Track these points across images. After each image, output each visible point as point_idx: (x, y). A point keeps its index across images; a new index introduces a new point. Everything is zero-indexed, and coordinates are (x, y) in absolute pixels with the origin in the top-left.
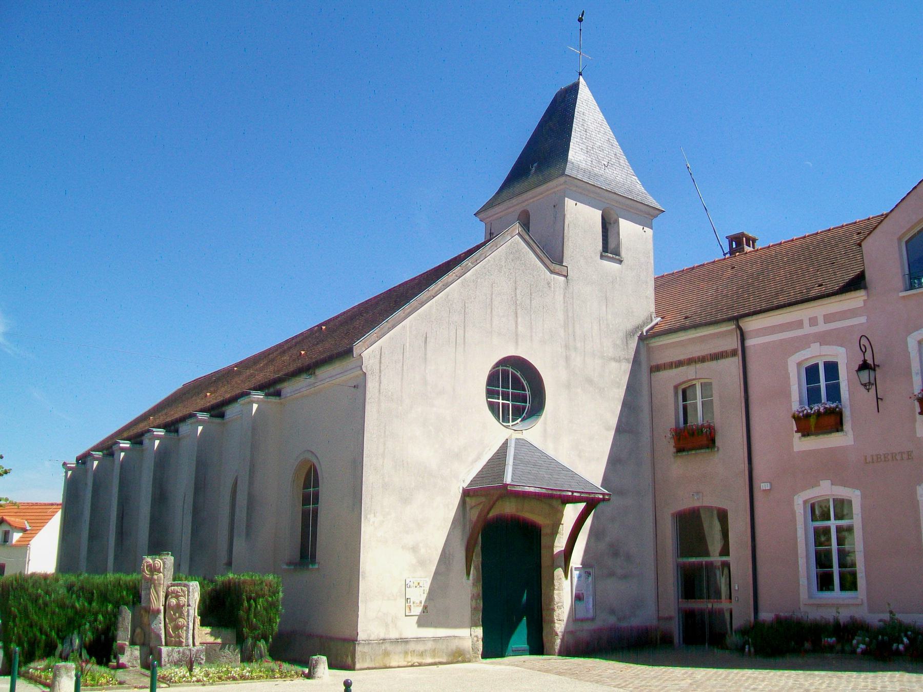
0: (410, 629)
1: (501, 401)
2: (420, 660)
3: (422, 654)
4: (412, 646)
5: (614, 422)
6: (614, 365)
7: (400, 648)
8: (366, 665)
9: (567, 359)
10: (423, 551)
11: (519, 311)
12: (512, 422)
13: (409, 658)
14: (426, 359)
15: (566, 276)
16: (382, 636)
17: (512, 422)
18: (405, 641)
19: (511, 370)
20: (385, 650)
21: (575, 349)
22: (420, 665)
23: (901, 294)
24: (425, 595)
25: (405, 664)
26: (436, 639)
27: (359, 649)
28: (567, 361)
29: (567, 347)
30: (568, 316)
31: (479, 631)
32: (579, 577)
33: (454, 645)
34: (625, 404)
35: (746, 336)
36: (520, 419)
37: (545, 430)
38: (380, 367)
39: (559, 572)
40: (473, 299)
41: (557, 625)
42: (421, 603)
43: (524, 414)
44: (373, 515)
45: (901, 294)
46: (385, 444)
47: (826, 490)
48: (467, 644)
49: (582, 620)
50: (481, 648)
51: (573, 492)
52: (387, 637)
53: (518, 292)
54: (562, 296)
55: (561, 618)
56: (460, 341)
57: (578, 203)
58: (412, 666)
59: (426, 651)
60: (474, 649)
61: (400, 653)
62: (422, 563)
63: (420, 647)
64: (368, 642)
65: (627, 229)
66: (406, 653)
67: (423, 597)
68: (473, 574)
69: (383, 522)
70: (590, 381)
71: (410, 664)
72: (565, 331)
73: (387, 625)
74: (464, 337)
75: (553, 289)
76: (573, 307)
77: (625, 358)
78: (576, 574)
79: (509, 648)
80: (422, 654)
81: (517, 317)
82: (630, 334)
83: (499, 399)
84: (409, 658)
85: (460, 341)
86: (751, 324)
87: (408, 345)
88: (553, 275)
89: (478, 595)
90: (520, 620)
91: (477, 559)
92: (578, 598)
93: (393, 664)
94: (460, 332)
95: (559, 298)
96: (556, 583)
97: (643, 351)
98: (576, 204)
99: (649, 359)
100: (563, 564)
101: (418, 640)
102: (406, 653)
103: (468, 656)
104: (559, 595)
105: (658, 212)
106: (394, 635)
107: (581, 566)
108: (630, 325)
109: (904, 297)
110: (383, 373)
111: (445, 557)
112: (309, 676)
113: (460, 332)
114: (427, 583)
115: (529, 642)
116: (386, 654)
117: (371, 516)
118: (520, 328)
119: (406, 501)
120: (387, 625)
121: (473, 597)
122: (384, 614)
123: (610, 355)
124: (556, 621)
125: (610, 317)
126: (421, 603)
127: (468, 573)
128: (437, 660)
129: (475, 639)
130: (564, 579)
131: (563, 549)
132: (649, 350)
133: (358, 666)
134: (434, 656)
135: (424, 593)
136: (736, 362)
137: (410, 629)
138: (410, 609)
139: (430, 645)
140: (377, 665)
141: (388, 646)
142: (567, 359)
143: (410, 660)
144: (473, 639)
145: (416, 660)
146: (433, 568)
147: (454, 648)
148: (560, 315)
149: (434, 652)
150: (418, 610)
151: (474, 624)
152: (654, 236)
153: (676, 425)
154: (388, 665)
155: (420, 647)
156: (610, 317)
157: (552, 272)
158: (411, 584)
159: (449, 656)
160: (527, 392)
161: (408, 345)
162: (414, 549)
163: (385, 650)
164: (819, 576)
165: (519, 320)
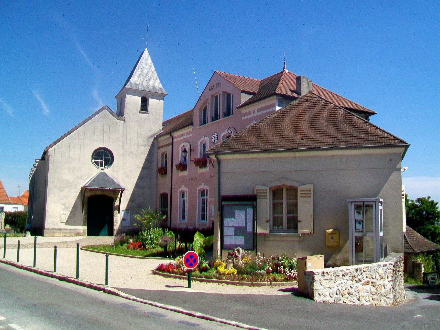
0: (63, 226)
1: (100, 161)
2: (65, 235)
3: (66, 233)
4: (62, 231)
5: (141, 165)
6: (143, 148)
7: (58, 231)
8: (47, 235)
9: (123, 147)
10: (67, 205)
11: (105, 134)
12: (104, 167)
13: (62, 234)
14: (70, 150)
15: (124, 121)
16: (53, 228)
17: (104, 167)
18: (60, 229)
19: (104, 151)
20: (54, 231)
21: (127, 143)
22: (65, 236)
23: (198, 127)
24: (67, 217)
25: (60, 235)
26: (71, 229)
27: (45, 231)
28: (123, 148)
29: (123, 143)
30: (124, 133)
31: (86, 228)
32: (124, 213)
33: (77, 231)
34: (146, 160)
35: (174, 138)
36: (107, 166)
37: (113, 169)
38: (54, 153)
39: (116, 212)
40: (87, 131)
41: (115, 227)
42: (66, 219)
43: (109, 164)
44: (51, 195)
45: (198, 127)
46: (55, 175)
47: (203, 186)
48: (82, 231)
49: (124, 226)
50: (87, 232)
51: (109, 188)
52: (54, 228)
53: (105, 127)
54: (122, 127)
55: (116, 225)
56: (82, 144)
57: (131, 96)
58: (62, 236)
59: (67, 232)
60: (84, 233)
61: (58, 233)
62: (67, 208)
63: (65, 231)
64: (48, 229)
65: (152, 102)
66: (60, 233)
67: (67, 218)
68: (84, 212)
69: (54, 197)
70: (132, 153)
71: (62, 236)
72: (123, 138)
73: (54, 225)
74: (84, 143)
75: (118, 125)
76: (127, 130)
77: (148, 145)
78: (123, 213)
79: (101, 234)
80: (66, 233)
81: (104, 135)
82: (151, 137)
83: (99, 160)
84: (62, 234)
85: (82, 144)
86: (175, 134)
87: (64, 146)
88: (119, 121)
89: (86, 218)
90: (105, 225)
91: (85, 208)
92: (123, 220)
93: (56, 235)
94: (82, 141)
95: (121, 128)
96: (115, 215)
97: (155, 142)
98: (130, 96)
99: (158, 144)
100: (118, 209)
101: (65, 229)
102: (60, 233)
103: (82, 234)
104: (116, 218)
105: (166, 95)
106: (57, 227)
107: (125, 210)
108: (151, 134)
109: (199, 128)
110: (55, 155)
111: (75, 207)
112: (25, 237)
113: (82, 141)
114: (68, 214)
115: (108, 232)
116: (54, 232)
117: (50, 196)
118: (105, 139)
119: (62, 191)
120: (54, 225)
121: (84, 218)
122: (54, 222)
123: (141, 144)
124: (114, 226)
125: (142, 132)
126: (66, 219)
127: (83, 211)
128: (71, 235)
129: (85, 230)
130: (118, 214)
131: (118, 205)
132: (158, 141)
133: (45, 235)
134: (70, 234)
135: (67, 216)
136: (171, 146)
137: (63, 226)
138: (62, 221)
139: (68, 231)
140: (51, 235)
141: (55, 231)
142: (123, 147)
143: (62, 234)
144: (83, 230)
145: (64, 235)
146: (70, 210)
147: (77, 232)
148: (121, 133)
149: (70, 233)
150: (65, 221)
151: (84, 225)
152: (164, 103)
153: (161, 166)
154: (54, 236)
155: (65, 231)
156: (142, 132)
157: (118, 120)
158: (63, 214)
159: (75, 234)
160: (110, 158)
161: (64, 146)
162: (64, 204)
163: (54, 231)
164: (86, 200)
165: (105, 136)
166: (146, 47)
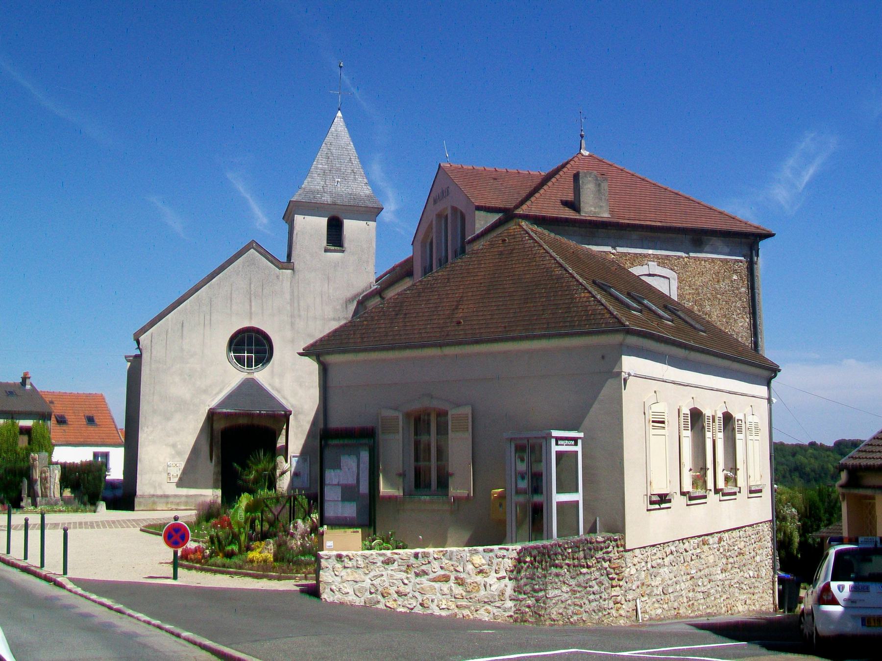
0: (172, 489)
1: (246, 355)
3: (178, 504)
4: (171, 500)
7: (164, 500)
8: (141, 509)
10: (179, 446)
11: (253, 298)
12: (255, 366)
14: (182, 336)
15: (293, 269)
16: (152, 492)
17: (255, 366)
18: (167, 496)
19: (254, 334)
20: (154, 500)
21: (300, 316)
24: (181, 471)
25: (166, 509)
26: (187, 496)
27: (137, 500)
29: (292, 316)
31: (219, 492)
32: (298, 462)
36: (261, 364)
42: (177, 475)
43: (264, 361)
44: (146, 428)
52: (155, 494)
53: (252, 285)
54: (289, 283)
58: (171, 510)
62: (179, 453)
64: (142, 496)
65: (350, 226)
66: (167, 503)
67: (179, 473)
71: (170, 509)
73: (155, 487)
74: (210, 319)
78: (294, 460)
81: (251, 301)
82: (350, 300)
87: (170, 330)
91: (217, 452)
93: (158, 509)
94: (208, 317)
95: (287, 285)
101: (175, 496)
106: (159, 492)
107: (298, 455)
108: (349, 294)
110: (153, 348)
111: (195, 450)
113: (208, 317)
114: (182, 465)
116: (154, 503)
117: (146, 429)
118: (253, 309)
120: (155, 487)
123: (330, 317)
125: (331, 291)
126: (177, 475)
128: (188, 508)
129: (216, 497)
130: (285, 463)
133: (136, 509)
134: (186, 506)
135: (179, 470)
137: (172, 489)
138: (170, 479)
139: (183, 499)
140: (148, 509)
141: (156, 499)
142: (292, 324)
145: (174, 507)
146: (187, 456)
147: (201, 501)
148: (288, 296)
149: (186, 503)
150: (176, 480)
151: (215, 487)
152: (377, 227)
155: (177, 500)
157: (280, 269)
158: (171, 465)
160: (267, 347)
161: (170, 330)
162: (174, 446)
164: (218, 437)
165: (253, 304)
166: (339, 110)
